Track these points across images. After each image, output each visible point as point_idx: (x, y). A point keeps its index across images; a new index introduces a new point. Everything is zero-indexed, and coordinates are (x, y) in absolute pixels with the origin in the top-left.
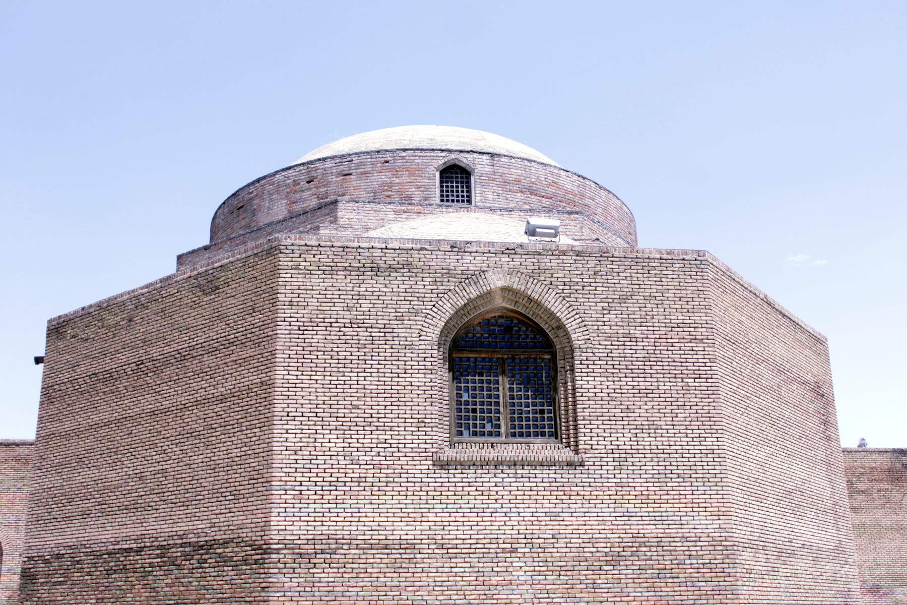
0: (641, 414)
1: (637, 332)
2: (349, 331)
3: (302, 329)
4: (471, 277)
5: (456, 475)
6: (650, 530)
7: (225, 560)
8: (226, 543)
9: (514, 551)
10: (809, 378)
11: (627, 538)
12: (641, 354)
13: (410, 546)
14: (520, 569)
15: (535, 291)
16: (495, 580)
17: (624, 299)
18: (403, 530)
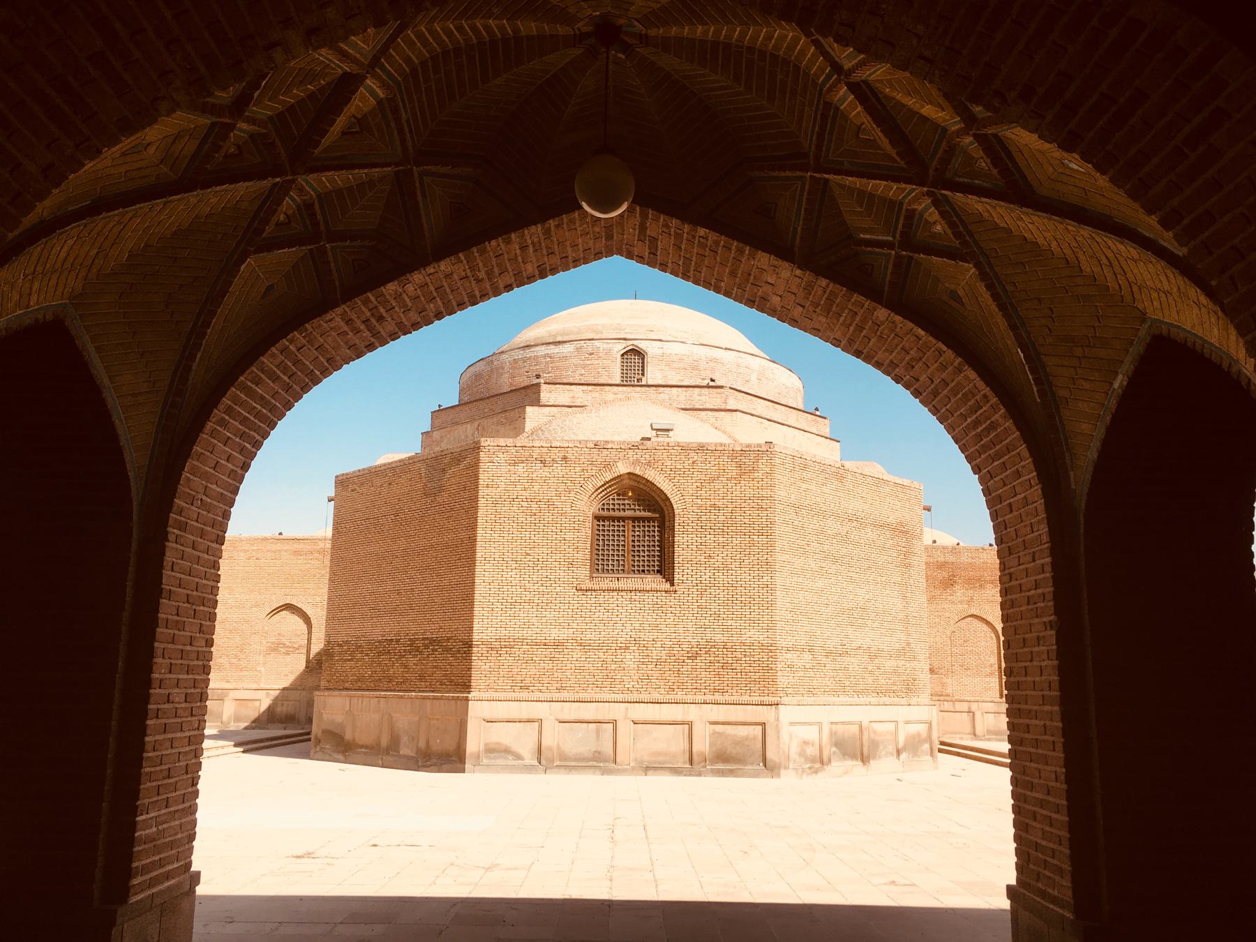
0: (718, 561)
1: (720, 504)
2: (525, 504)
3: (495, 503)
4: (607, 466)
5: (591, 598)
6: (719, 638)
7: (447, 650)
8: (448, 639)
9: (627, 648)
10: (892, 520)
11: (703, 642)
12: (722, 518)
13: (558, 644)
14: (630, 659)
15: (651, 475)
16: (613, 667)
17: (712, 480)
18: (555, 634)
